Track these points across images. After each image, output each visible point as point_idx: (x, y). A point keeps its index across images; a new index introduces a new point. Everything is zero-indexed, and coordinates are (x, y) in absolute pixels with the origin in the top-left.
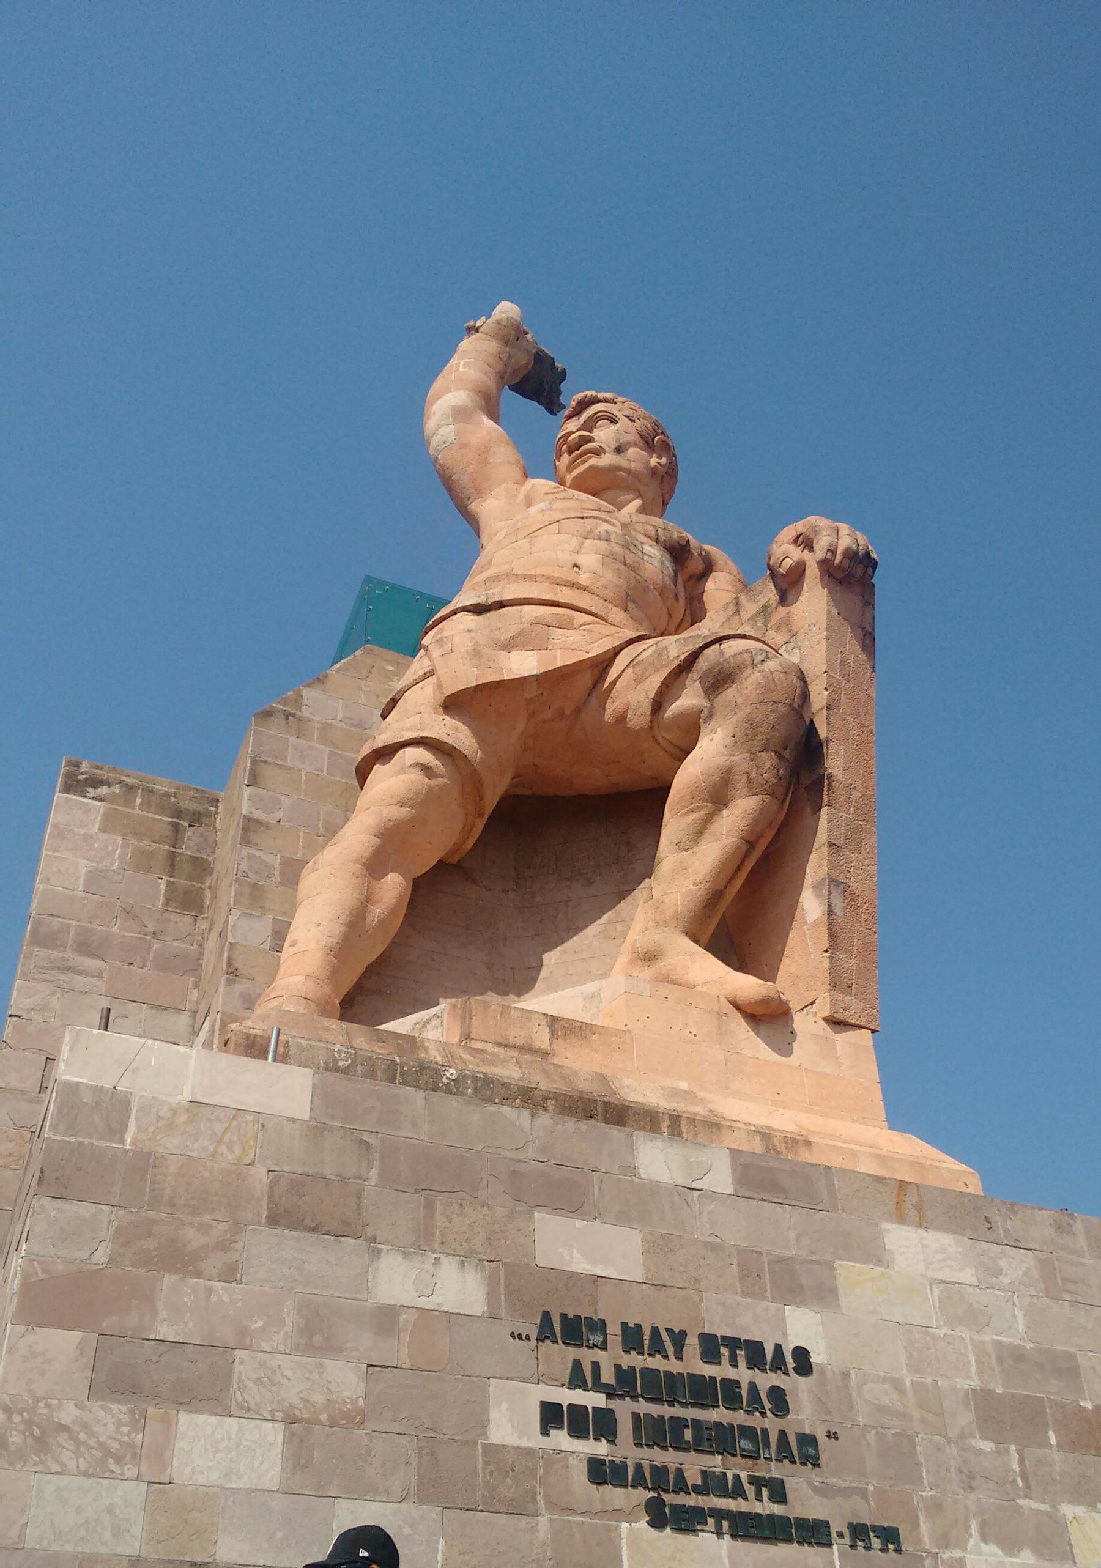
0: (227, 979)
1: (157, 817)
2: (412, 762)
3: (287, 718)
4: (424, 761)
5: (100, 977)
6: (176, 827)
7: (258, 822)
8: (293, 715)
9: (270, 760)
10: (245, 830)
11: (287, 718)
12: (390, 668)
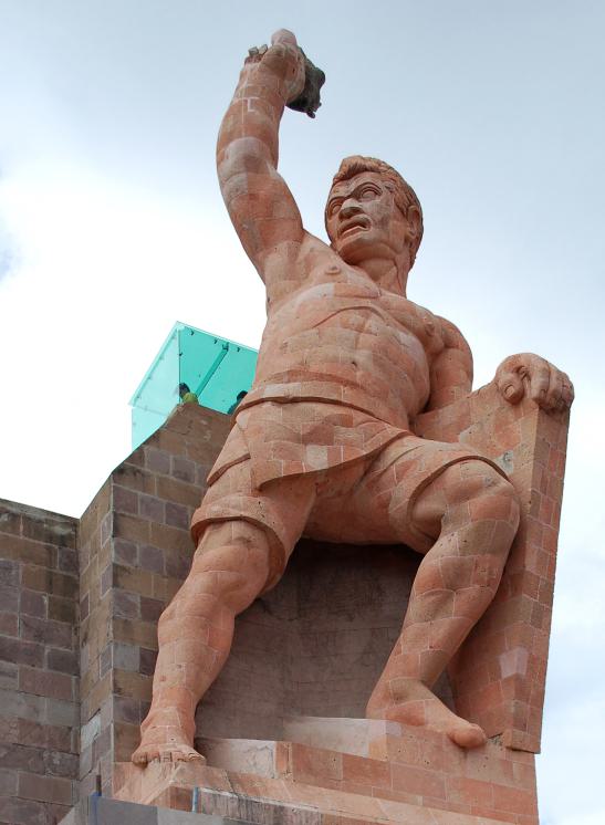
0: (115, 697)
1: (37, 542)
2: (237, 536)
3: (135, 474)
4: (246, 536)
5: (14, 676)
6: (48, 549)
7: (124, 569)
8: (139, 471)
9: (127, 514)
10: (115, 576)
11: (135, 474)
12: (204, 422)
